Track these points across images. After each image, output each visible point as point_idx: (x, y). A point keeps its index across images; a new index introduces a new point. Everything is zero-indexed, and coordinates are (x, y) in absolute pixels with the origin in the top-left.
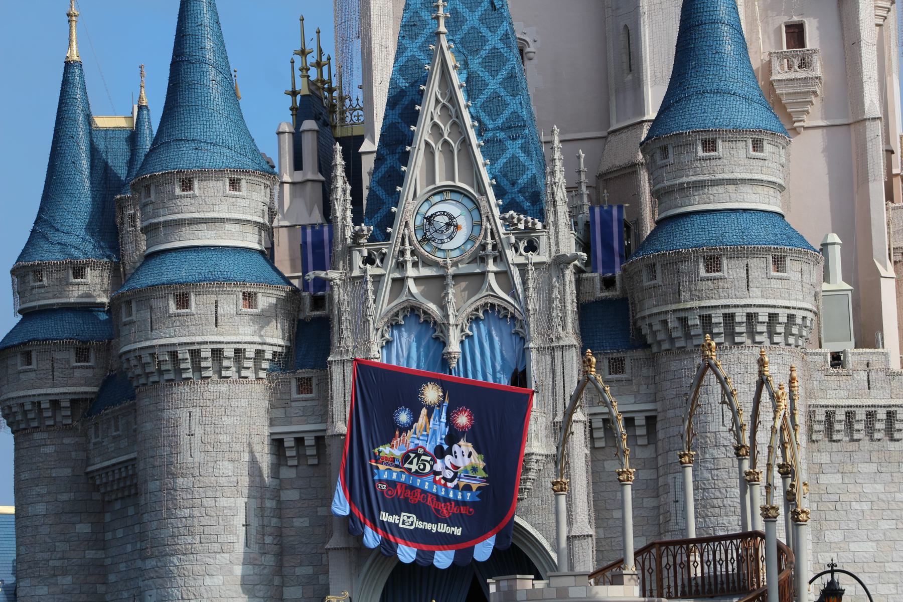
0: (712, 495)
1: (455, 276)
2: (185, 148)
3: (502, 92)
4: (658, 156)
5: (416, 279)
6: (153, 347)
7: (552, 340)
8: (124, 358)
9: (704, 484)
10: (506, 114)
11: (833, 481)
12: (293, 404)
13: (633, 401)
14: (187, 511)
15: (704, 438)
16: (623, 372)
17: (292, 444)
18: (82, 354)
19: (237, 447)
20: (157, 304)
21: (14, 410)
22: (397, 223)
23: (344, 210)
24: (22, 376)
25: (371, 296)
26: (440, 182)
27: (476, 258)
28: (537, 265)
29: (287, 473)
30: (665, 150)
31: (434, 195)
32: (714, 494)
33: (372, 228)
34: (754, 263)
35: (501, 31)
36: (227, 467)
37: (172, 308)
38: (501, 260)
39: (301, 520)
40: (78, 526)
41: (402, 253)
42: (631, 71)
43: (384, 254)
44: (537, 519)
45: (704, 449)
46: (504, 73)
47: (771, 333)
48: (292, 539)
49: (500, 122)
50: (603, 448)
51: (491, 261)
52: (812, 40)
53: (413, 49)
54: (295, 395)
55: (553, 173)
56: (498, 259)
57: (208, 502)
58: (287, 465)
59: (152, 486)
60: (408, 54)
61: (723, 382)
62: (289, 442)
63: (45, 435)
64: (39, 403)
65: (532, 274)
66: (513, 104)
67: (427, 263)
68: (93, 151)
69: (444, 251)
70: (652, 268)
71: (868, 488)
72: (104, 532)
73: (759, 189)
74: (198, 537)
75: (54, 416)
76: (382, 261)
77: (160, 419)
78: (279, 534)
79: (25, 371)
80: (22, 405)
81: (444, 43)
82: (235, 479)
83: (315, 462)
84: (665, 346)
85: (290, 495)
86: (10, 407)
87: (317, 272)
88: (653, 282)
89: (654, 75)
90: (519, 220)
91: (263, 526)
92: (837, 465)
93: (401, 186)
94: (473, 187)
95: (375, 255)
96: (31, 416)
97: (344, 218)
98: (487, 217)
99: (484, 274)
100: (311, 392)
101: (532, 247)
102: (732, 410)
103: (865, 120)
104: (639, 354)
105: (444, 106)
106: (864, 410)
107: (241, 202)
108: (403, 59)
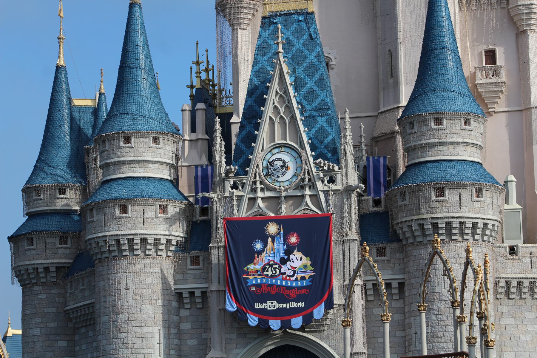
0: (437, 330)
1: (286, 197)
2: (127, 118)
3: (316, 88)
4: (408, 128)
5: (263, 198)
6: (106, 236)
7: (343, 236)
8: (88, 243)
9: (433, 323)
10: (318, 101)
11: (509, 323)
12: (189, 272)
13: (391, 273)
14: (124, 335)
15: (433, 296)
16: (385, 256)
17: (187, 295)
18: (63, 240)
19: (155, 297)
20: (108, 211)
21: (22, 272)
22: (252, 165)
23: (221, 157)
24: (27, 252)
25: (235, 208)
27: (299, 186)
28: (335, 191)
29: (184, 313)
30: (412, 124)
31: (274, 148)
32: (438, 329)
33: (237, 168)
34: (464, 192)
35: (315, 52)
36: (148, 309)
37: (118, 213)
38: (314, 188)
39: (192, 341)
40: (59, 342)
41: (255, 183)
42: (392, 77)
43: (244, 183)
44: (333, 342)
45: (433, 302)
46: (317, 77)
47: (474, 234)
48: (186, 352)
49: (314, 106)
50: (373, 301)
51: (307, 189)
52: (500, 60)
53: (263, 62)
54: (190, 267)
55: (345, 137)
56: (312, 187)
57: (137, 329)
58: (184, 308)
59: (104, 319)
60: (260, 65)
61: (444, 262)
62: (186, 294)
63: (41, 288)
64: (37, 269)
65: (331, 197)
66: (322, 96)
67: (270, 189)
68: (72, 119)
69: (280, 182)
70: (403, 194)
71: (530, 327)
72: (75, 346)
73: (468, 148)
74: (130, 350)
75: (46, 277)
76: (242, 188)
77: (109, 279)
78: (179, 350)
79: (29, 250)
80: (27, 270)
81: (282, 58)
82: (153, 316)
83: (201, 306)
84: (410, 241)
85: (186, 326)
86: (20, 271)
87: (204, 193)
88: (404, 202)
89: (406, 80)
90: (325, 164)
91: (169, 344)
92: (512, 313)
93: (255, 143)
94: (297, 144)
95: (238, 184)
96: (32, 276)
97: (220, 162)
98: (306, 162)
99: (303, 196)
100: (199, 265)
101: (332, 180)
102: (450, 279)
103: (531, 108)
104: (395, 245)
105: (281, 96)
106: (528, 281)
107: (159, 151)
108: (257, 68)
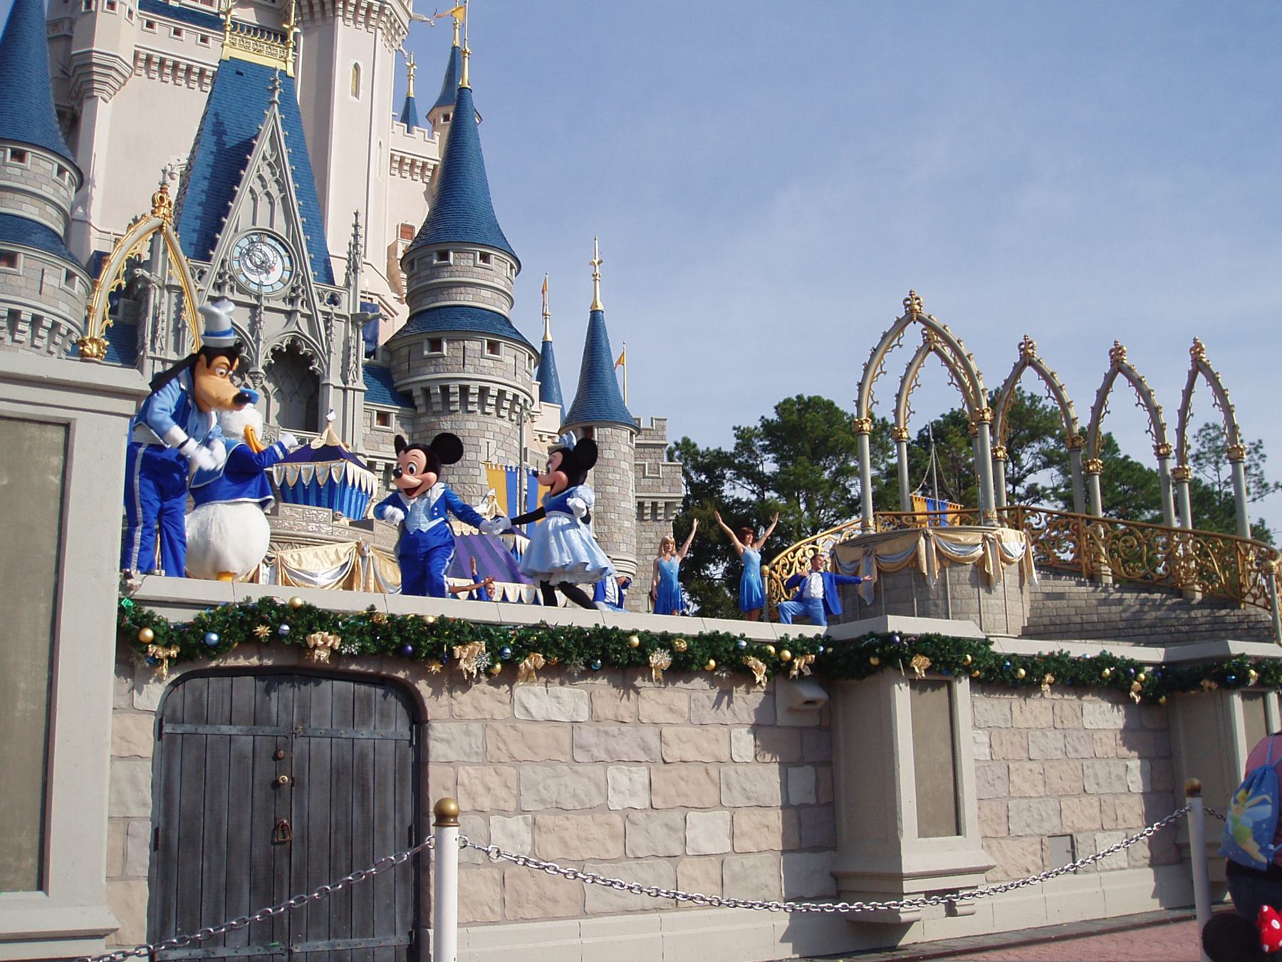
26: (263, 223)
67: (242, 290)
76: (199, 278)
101: (334, 300)
